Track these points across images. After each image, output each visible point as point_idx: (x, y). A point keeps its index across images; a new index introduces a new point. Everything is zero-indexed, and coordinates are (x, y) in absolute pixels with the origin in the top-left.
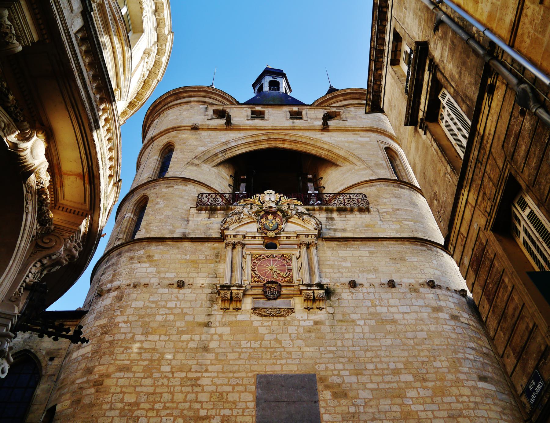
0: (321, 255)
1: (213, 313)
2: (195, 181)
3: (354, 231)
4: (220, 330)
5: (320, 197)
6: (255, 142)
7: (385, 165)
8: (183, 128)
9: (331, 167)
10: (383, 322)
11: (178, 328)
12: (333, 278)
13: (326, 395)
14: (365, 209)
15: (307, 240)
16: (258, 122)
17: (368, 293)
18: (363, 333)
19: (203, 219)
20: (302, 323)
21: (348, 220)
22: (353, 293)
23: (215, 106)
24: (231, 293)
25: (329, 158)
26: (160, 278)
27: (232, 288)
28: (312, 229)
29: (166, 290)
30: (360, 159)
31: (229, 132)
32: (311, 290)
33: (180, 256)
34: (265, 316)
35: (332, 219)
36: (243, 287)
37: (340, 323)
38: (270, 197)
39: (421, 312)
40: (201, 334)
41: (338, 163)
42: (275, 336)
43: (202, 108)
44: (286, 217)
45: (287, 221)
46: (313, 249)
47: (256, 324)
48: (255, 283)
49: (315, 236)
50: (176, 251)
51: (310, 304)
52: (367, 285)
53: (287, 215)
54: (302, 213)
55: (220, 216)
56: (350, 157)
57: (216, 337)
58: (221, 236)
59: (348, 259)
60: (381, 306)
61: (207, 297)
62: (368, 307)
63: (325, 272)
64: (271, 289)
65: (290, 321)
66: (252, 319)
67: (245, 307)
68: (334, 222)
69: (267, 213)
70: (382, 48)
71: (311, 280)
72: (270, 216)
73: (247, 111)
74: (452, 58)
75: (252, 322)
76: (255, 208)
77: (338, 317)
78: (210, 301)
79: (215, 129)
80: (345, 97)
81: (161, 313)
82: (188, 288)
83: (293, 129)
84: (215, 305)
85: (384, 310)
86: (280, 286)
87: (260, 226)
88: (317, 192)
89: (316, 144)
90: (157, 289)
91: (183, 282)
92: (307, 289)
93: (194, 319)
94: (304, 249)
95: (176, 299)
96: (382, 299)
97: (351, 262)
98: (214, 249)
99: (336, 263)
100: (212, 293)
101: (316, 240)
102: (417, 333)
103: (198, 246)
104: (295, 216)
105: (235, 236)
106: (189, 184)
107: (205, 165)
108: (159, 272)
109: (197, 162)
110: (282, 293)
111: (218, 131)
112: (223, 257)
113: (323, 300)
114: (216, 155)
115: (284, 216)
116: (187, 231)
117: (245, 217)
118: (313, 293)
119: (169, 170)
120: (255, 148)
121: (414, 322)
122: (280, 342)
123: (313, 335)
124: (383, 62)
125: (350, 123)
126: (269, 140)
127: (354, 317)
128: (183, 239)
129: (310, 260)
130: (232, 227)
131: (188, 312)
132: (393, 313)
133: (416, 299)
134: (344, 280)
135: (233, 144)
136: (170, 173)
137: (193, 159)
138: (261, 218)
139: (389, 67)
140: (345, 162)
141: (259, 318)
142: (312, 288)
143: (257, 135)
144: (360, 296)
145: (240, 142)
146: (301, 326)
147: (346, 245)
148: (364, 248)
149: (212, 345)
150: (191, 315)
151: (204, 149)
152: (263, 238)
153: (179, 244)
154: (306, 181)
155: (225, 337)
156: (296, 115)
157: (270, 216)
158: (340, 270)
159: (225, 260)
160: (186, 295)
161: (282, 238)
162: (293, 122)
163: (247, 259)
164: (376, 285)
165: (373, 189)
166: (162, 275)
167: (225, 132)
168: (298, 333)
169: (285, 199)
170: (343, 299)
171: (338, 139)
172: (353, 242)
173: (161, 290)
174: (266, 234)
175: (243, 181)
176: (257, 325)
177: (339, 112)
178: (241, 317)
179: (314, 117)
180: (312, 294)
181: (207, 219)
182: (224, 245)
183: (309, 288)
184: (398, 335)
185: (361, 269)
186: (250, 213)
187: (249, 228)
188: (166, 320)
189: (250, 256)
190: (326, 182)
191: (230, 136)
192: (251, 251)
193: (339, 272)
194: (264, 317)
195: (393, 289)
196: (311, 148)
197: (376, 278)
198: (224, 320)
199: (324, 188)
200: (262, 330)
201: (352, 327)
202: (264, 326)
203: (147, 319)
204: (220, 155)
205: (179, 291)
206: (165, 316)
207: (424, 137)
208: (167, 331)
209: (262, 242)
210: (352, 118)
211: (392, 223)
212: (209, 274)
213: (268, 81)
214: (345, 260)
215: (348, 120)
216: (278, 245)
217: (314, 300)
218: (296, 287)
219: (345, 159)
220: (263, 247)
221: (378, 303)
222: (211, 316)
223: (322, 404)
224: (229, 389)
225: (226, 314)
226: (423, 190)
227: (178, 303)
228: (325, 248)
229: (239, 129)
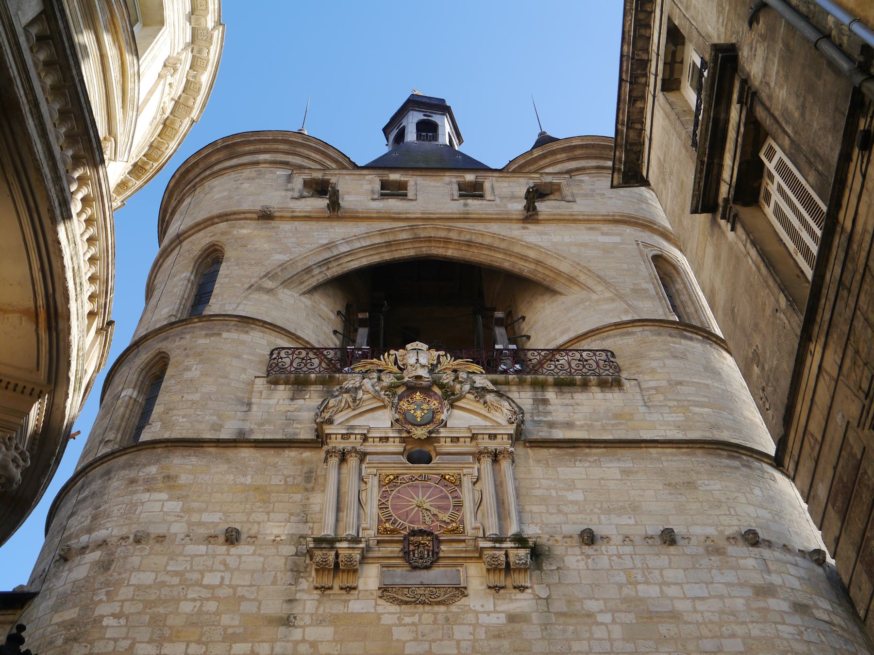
0: (522, 476)
1: (298, 597)
2: (265, 322)
3: (590, 427)
4: (312, 633)
5: (518, 356)
6: (388, 244)
7: (653, 292)
8: (242, 216)
9: (542, 295)
10: (651, 618)
11: (225, 628)
12: (547, 525)
14: (611, 381)
15: (492, 445)
16: (394, 204)
17: (619, 556)
18: (611, 640)
19: (281, 402)
20: (484, 619)
21: (577, 404)
22: (588, 557)
23: (307, 171)
24: (337, 556)
25: (539, 277)
26: (190, 524)
27: (338, 545)
28: (504, 422)
29: (202, 549)
30: (601, 279)
31: (334, 223)
32: (500, 549)
33: (231, 477)
34: (406, 603)
35: (545, 402)
36: (360, 542)
37: (562, 620)
38: (418, 358)
39: (730, 596)
40: (273, 641)
41: (557, 287)
42: (426, 646)
43: (280, 176)
44: (451, 397)
45: (452, 406)
46: (505, 464)
47: (386, 620)
48: (386, 534)
49: (510, 436)
50: (224, 467)
51: (499, 579)
52: (617, 539)
53: (453, 394)
54: (484, 389)
55: (315, 395)
58: (318, 436)
60: (647, 583)
61: (286, 564)
62: (620, 586)
63: (531, 511)
64: (420, 548)
65: (458, 613)
66: (380, 609)
67: (366, 584)
68: (550, 408)
69: (411, 389)
70: (644, 57)
71: (501, 528)
72: (418, 396)
73: (372, 182)
74: (786, 77)
75: (379, 616)
76: (387, 380)
77: (559, 606)
78: (292, 570)
79: (307, 218)
80: (571, 155)
81: (190, 596)
82: (248, 544)
83: (465, 218)
84: (303, 580)
85: (654, 591)
86: (437, 541)
87: (397, 416)
88: (514, 347)
89: (511, 248)
90: (184, 545)
91: (238, 532)
92: (494, 548)
93: (259, 608)
94: (486, 463)
95: (222, 568)
96: (648, 568)
97: (585, 491)
98: (303, 462)
99: (554, 493)
100: (296, 555)
101: (512, 445)
102: (724, 641)
103: (270, 456)
104: (469, 396)
106: (252, 329)
108: (187, 510)
109: (269, 284)
110: (441, 555)
111: (314, 223)
112: (321, 480)
113: (526, 570)
114: (308, 270)
115: (446, 396)
116: (247, 426)
117: (365, 397)
118: (507, 555)
119: (212, 300)
120: (387, 257)
121: (716, 618)
123: (506, 643)
124: (646, 84)
125: (581, 207)
126: (417, 239)
127: (592, 605)
128: (239, 442)
129: (499, 486)
130: (339, 418)
131: (247, 595)
132: (672, 599)
133: (719, 568)
134: (567, 529)
135: (344, 249)
136: (214, 307)
137: (261, 278)
138: (400, 400)
139: (660, 95)
140: (571, 285)
141: (394, 608)
142: (504, 545)
143: (392, 231)
144: (604, 562)
145: (358, 245)
146: (482, 626)
147: (573, 455)
148: (611, 461)
150: (254, 600)
151: (283, 258)
152: (403, 440)
153: (230, 453)
154: (490, 323)
156: (473, 191)
157: (418, 396)
158: (563, 508)
159: (324, 486)
160: (243, 559)
161: (443, 440)
162: (466, 205)
163: (369, 485)
164: (637, 540)
165: (629, 340)
166: (195, 518)
167: (327, 224)
168: (475, 640)
169: (448, 361)
170: (568, 569)
171: (556, 239)
172: (587, 450)
173: (191, 549)
174: (409, 432)
175: (363, 323)
176: (390, 622)
177: (559, 184)
178: (356, 606)
179: (509, 194)
180: (503, 558)
181: (287, 402)
182: (322, 455)
183: (497, 545)
184: (683, 646)
185: (605, 505)
186: (377, 388)
187: (374, 419)
188: (200, 612)
189: (376, 479)
191: (338, 232)
192: (378, 468)
193: (560, 511)
194: (403, 606)
195: (672, 549)
196: (501, 256)
197: (636, 524)
198: (321, 611)
199: (529, 337)
200: (399, 633)
201: (587, 628)
202: (405, 625)
203: (161, 610)
204: (316, 271)
205: (228, 550)
206: (198, 604)
207: (731, 235)
208: (202, 635)
209: (402, 449)
210: (585, 196)
211: (667, 410)
212: (291, 514)
213: (416, 121)
214: (571, 485)
215: (578, 200)
216: (433, 454)
217: (508, 569)
218: (471, 542)
219: (571, 280)
220: (404, 459)
221: (640, 578)
222: (295, 604)
225: (325, 599)
226: (731, 345)
227: (227, 576)
228: (531, 461)
229: (355, 217)
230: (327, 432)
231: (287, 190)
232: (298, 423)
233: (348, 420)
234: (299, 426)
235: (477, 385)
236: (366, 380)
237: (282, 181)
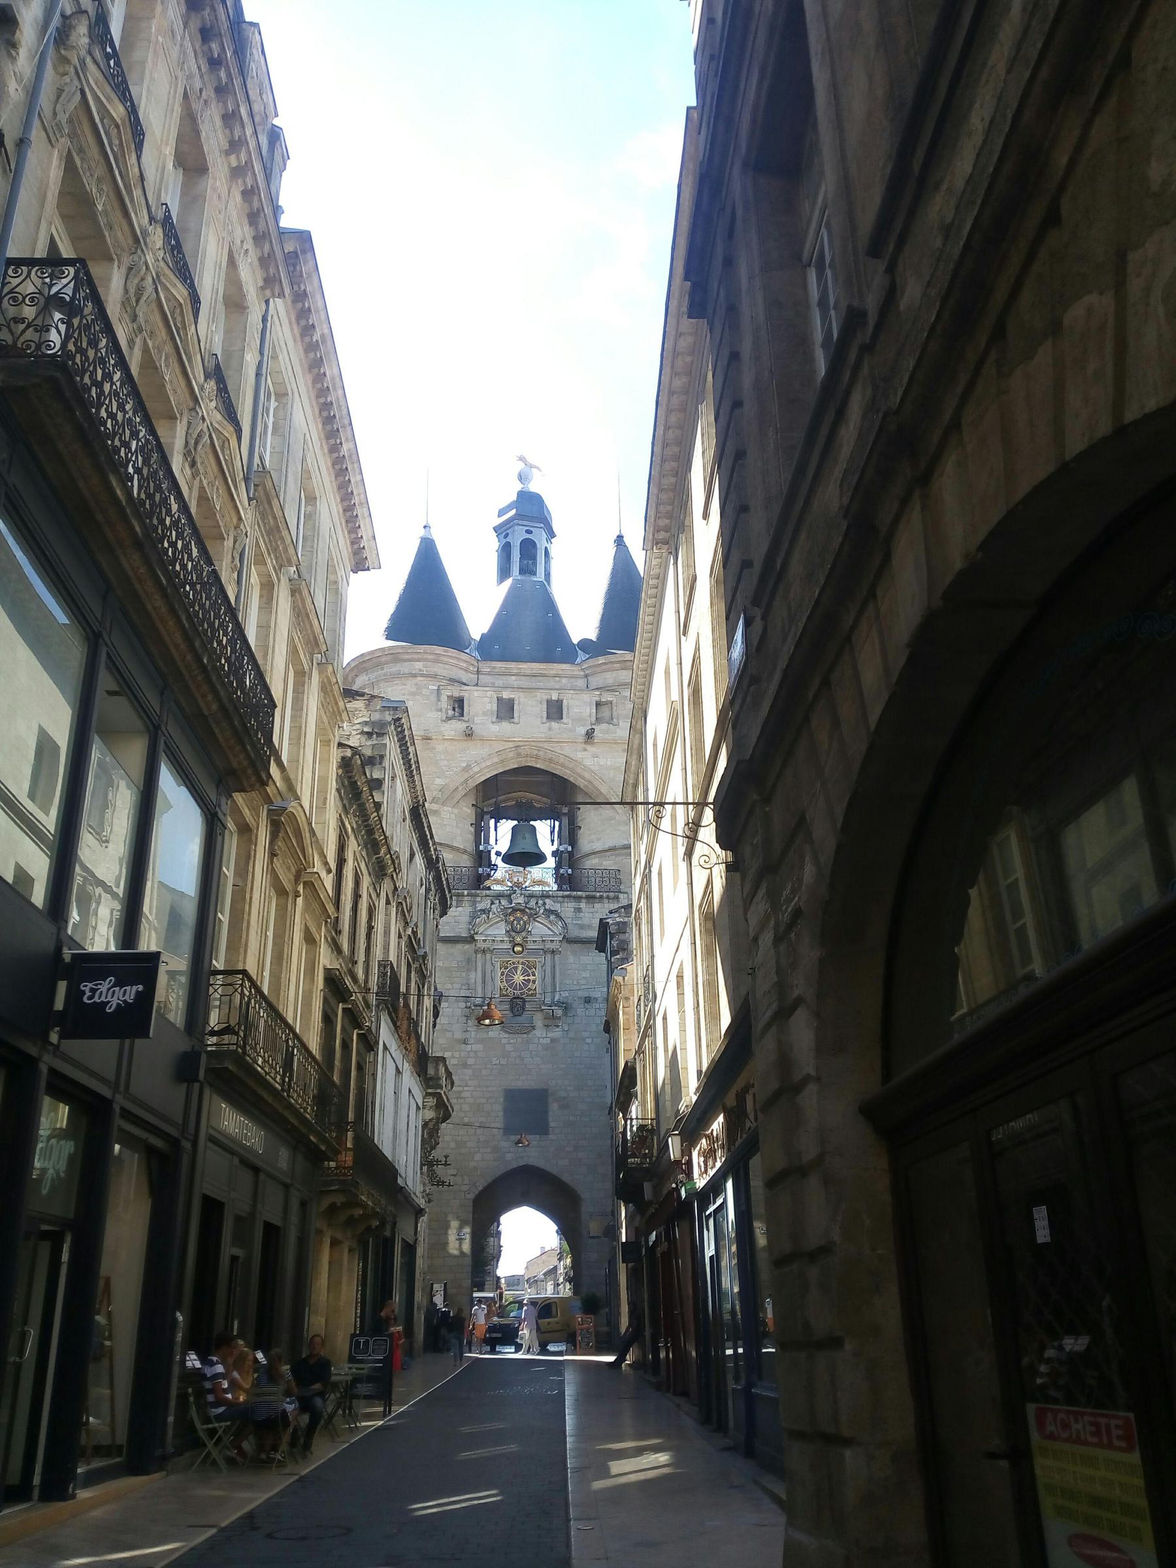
4: (476, 1047)
13: (554, 1107)
15: (549, 946)
35: (579, 910)
44: (533, 916)
51: (547, 1022)
57: (472, 1054)
59: (589, 967)
72: (518, 914)
77: (572, 1034)
86: (524, 1001)
122: (522, 1059)
127: (585, 1034)
134: (580, 994)
135: (476, 769)
144: (592, 1012)
149: (470, 1061)
155: (480, 1054)
157: (518, 914)
162: (550, 729)
175: (487, 813)
200: (508, 1048)
223: (550, 1113)
224: (484, 1101)
237: (433, 698)
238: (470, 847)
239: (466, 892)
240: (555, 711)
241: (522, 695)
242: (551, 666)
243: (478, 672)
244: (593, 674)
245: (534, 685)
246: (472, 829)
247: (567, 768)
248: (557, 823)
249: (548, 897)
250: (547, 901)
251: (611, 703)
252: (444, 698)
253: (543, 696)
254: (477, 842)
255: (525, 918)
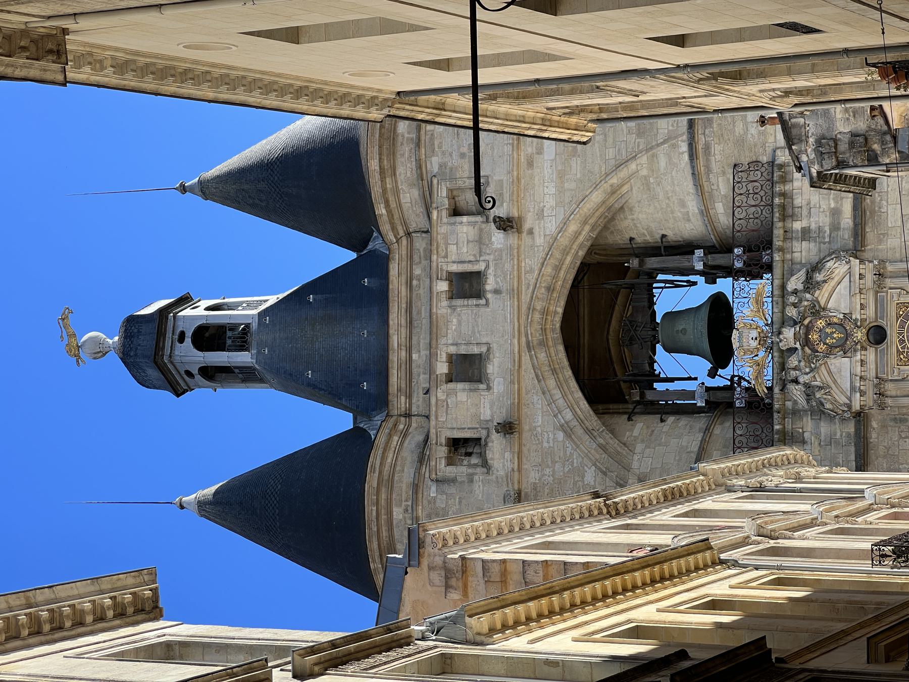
0: (898, 255)
15: (870, 278)
21: (809, 204)
25: (602, 222)
28: (847, 267)
44: (817, 310)
55: (799, 424)
56: (611, 182)
68: (813, 226)
69: (807, 342)
98: (884, 426)
104: (816, 295)
105: (863, 394)
107: (635, 465)
114: (603, 448)
130: (843, 399)
135: (569, 415)
147: (873, 212)
157: (814, 337)
161: (863, 317)
162: (497, 292)
165: (717, 149)
171: (550, 202)
175: (642, 395)
186: (807, 370)
190: (651, 234)
204: (601, 441)
219: (613, 192)
230: (858, 408)
231: (471, 481)
232: (835, 435)
233: (843, 392)
234: (838, 434)
235: (800, 287)
236: (801, 380)
237: (452, 490)
238: (700, 422)
239: (777, 427)
240: (467, 285)
241: (443, 341)
242: (393, 296)
243: (408, 415)
244: (405, 224)
245: (425, 322)
246: (671, 419)
247: (562, 262)
248: (660, 277)
249: (783, 287)
250: (790, 287)
251: (450, 191)
252: (451, 471)
253: (442, 307)
254: (691, 411)
255: (821, 323)
